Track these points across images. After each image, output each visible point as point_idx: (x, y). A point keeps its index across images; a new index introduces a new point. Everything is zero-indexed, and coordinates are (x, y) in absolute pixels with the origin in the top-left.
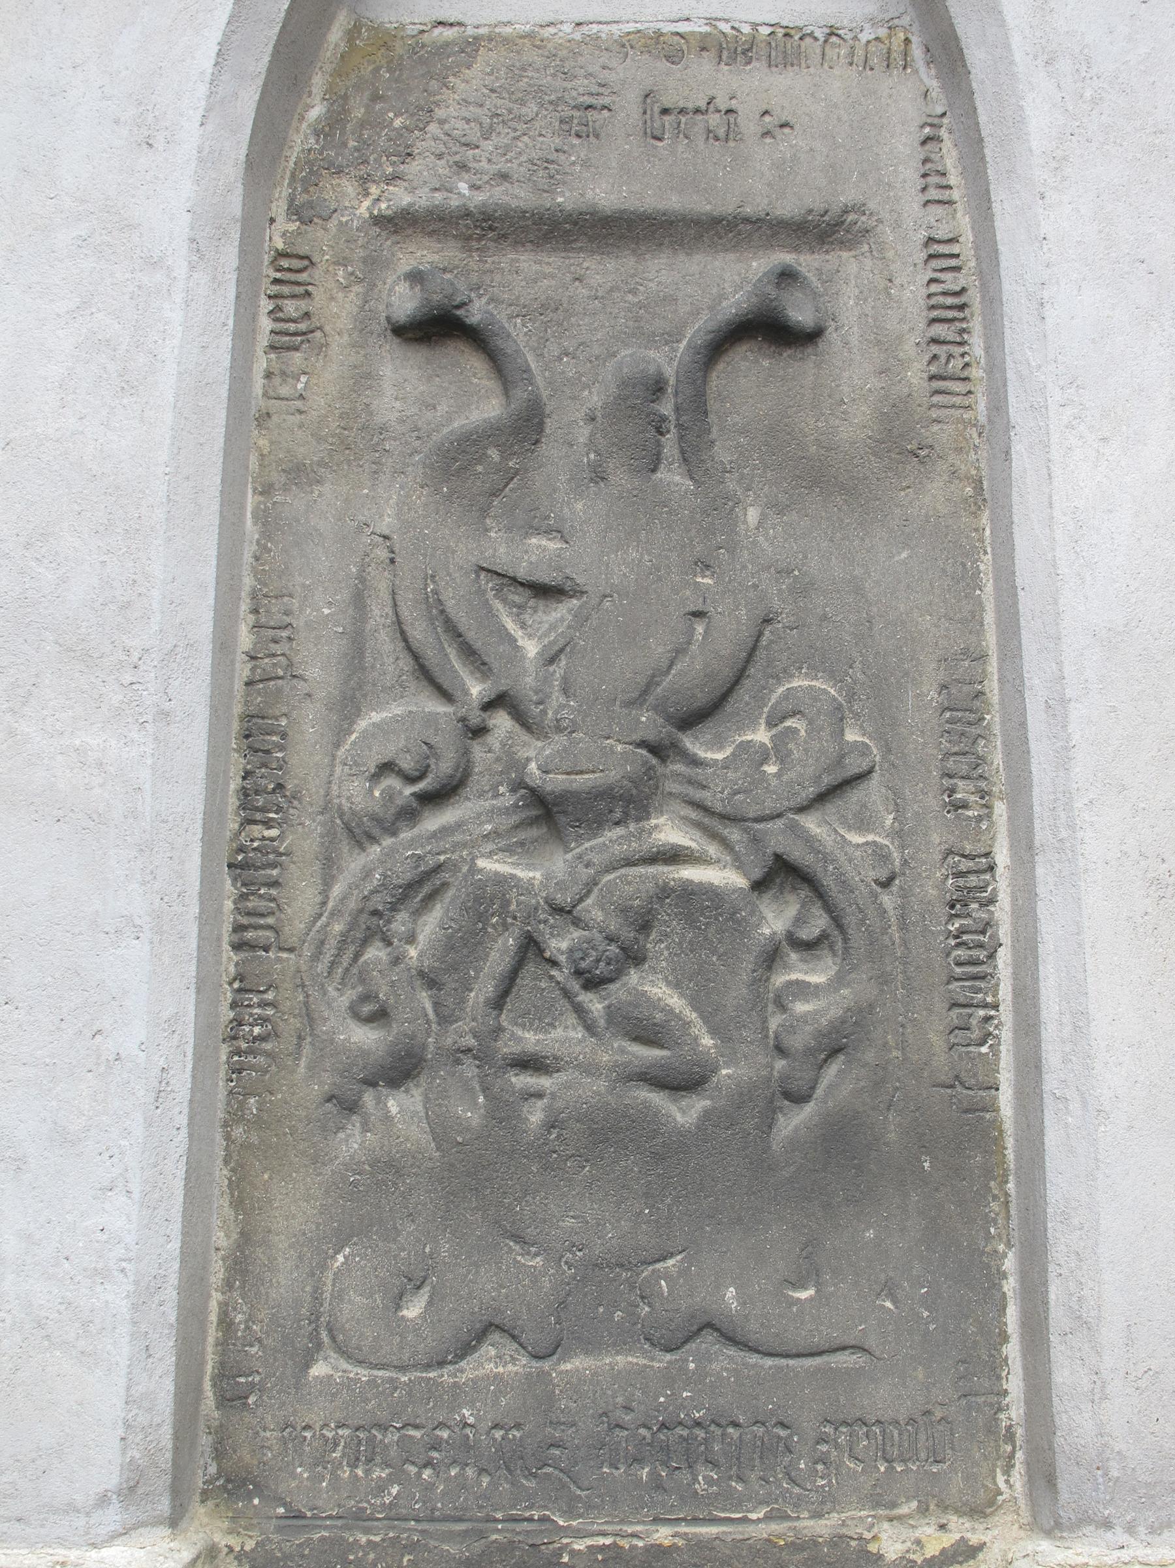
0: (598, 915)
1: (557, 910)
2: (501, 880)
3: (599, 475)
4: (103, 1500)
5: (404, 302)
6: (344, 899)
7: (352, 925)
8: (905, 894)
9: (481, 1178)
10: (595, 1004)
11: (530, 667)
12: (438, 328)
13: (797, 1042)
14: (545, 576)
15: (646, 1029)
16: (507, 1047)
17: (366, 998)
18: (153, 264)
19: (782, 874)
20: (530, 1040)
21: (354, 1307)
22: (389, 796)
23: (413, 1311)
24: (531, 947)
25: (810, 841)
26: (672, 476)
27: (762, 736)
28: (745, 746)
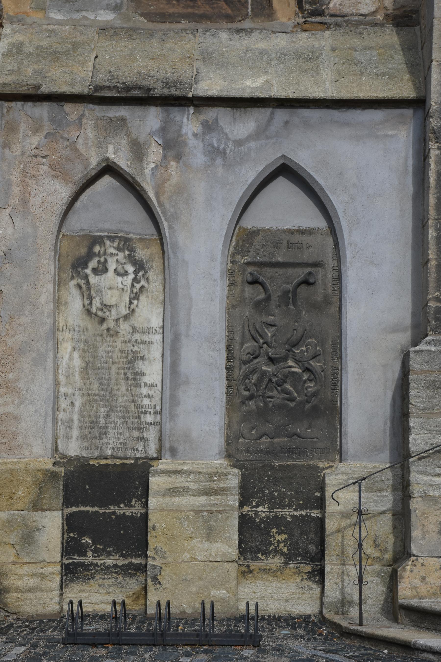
0: (280, 376)
1: (274, 375)
2: (266, 371)
3: (280, 306)
4: (216, 455)
5: (250, 279)
6: (243, 373)
7: (244, 377)
8: (325, 373)
9: (262, 414)
10: (279, 389)
11: (269, 338)
12: (254, 282)
13: (309, 395)
14: (273, 323)
15: (287, 392)
16: (266, 395)
17: (246, 387)
18: (215, 281)
19: (307, 370)
20: (270, 394)
21: (245, 431)
22: (249, 358)
23: (253, 432)
24: (270, 380)
25: (311, 365)
26: (291, 307)
27: (304, 349)
28: (302, 350)
